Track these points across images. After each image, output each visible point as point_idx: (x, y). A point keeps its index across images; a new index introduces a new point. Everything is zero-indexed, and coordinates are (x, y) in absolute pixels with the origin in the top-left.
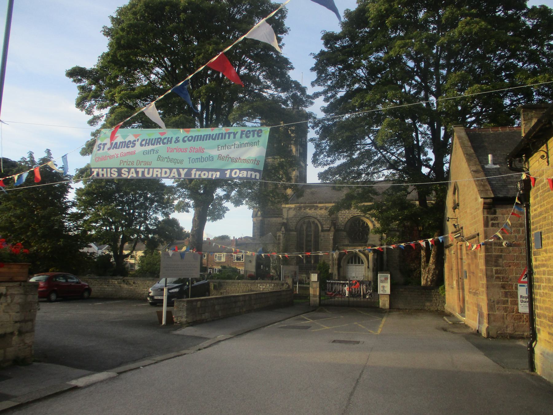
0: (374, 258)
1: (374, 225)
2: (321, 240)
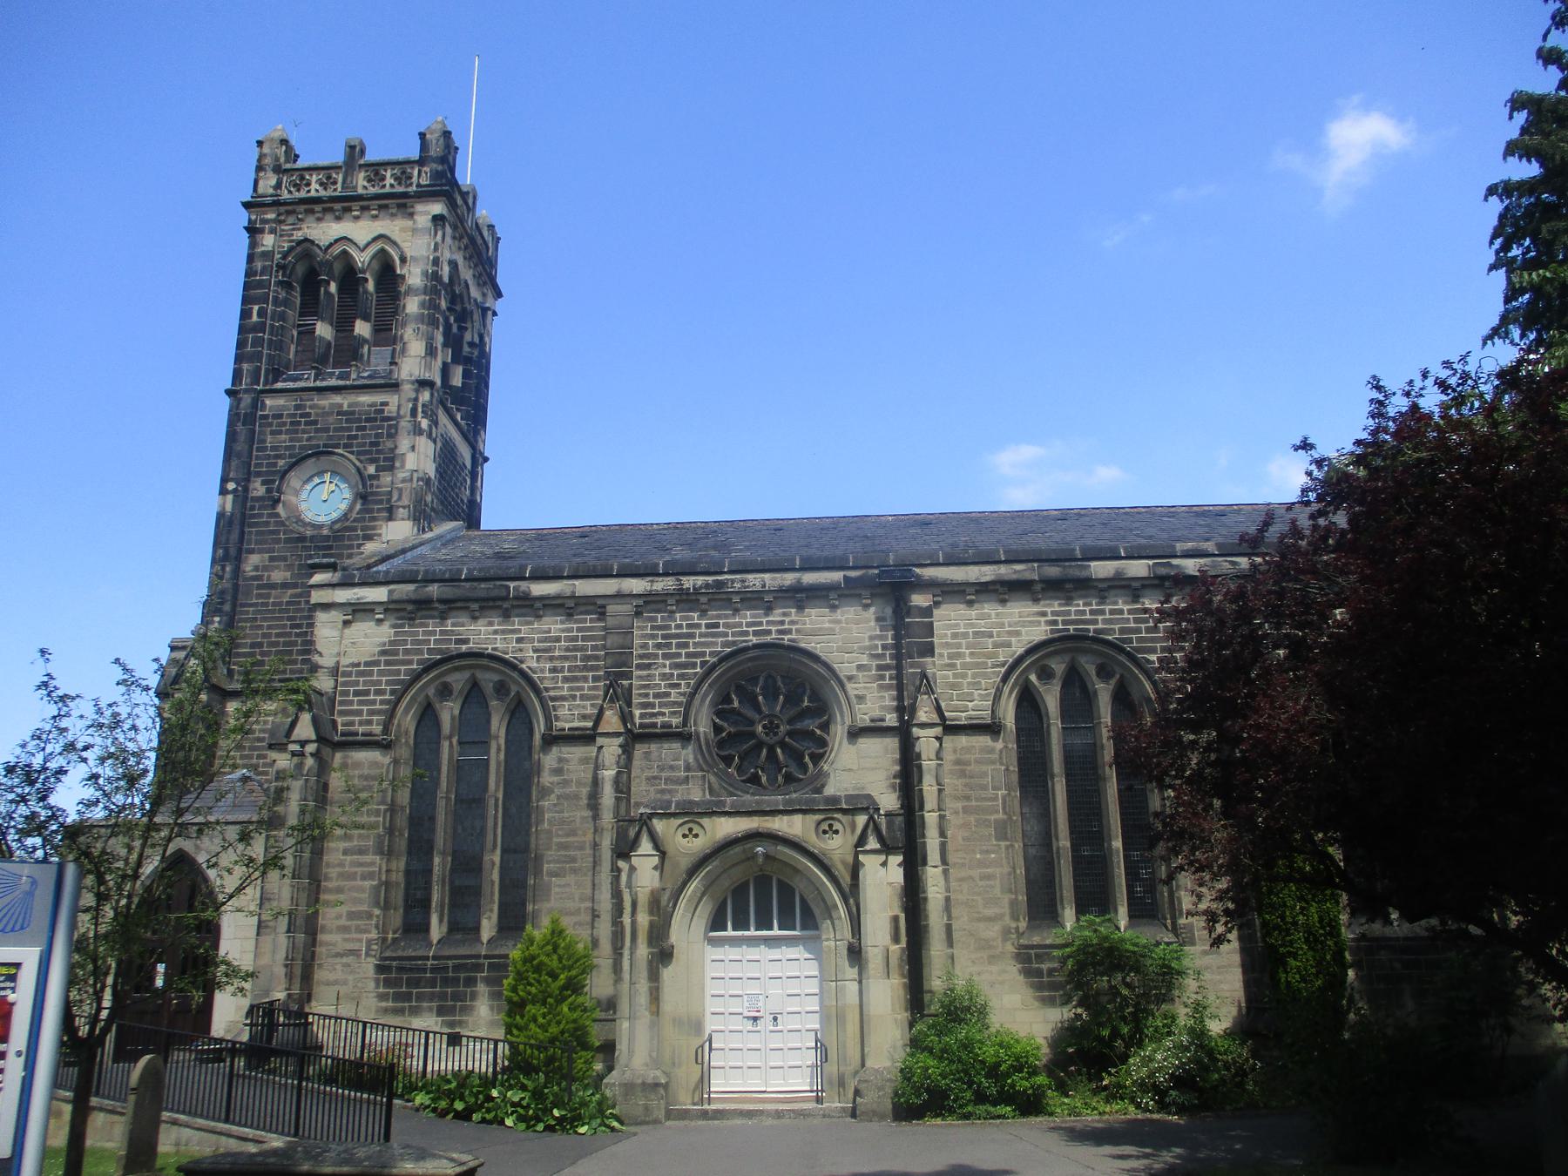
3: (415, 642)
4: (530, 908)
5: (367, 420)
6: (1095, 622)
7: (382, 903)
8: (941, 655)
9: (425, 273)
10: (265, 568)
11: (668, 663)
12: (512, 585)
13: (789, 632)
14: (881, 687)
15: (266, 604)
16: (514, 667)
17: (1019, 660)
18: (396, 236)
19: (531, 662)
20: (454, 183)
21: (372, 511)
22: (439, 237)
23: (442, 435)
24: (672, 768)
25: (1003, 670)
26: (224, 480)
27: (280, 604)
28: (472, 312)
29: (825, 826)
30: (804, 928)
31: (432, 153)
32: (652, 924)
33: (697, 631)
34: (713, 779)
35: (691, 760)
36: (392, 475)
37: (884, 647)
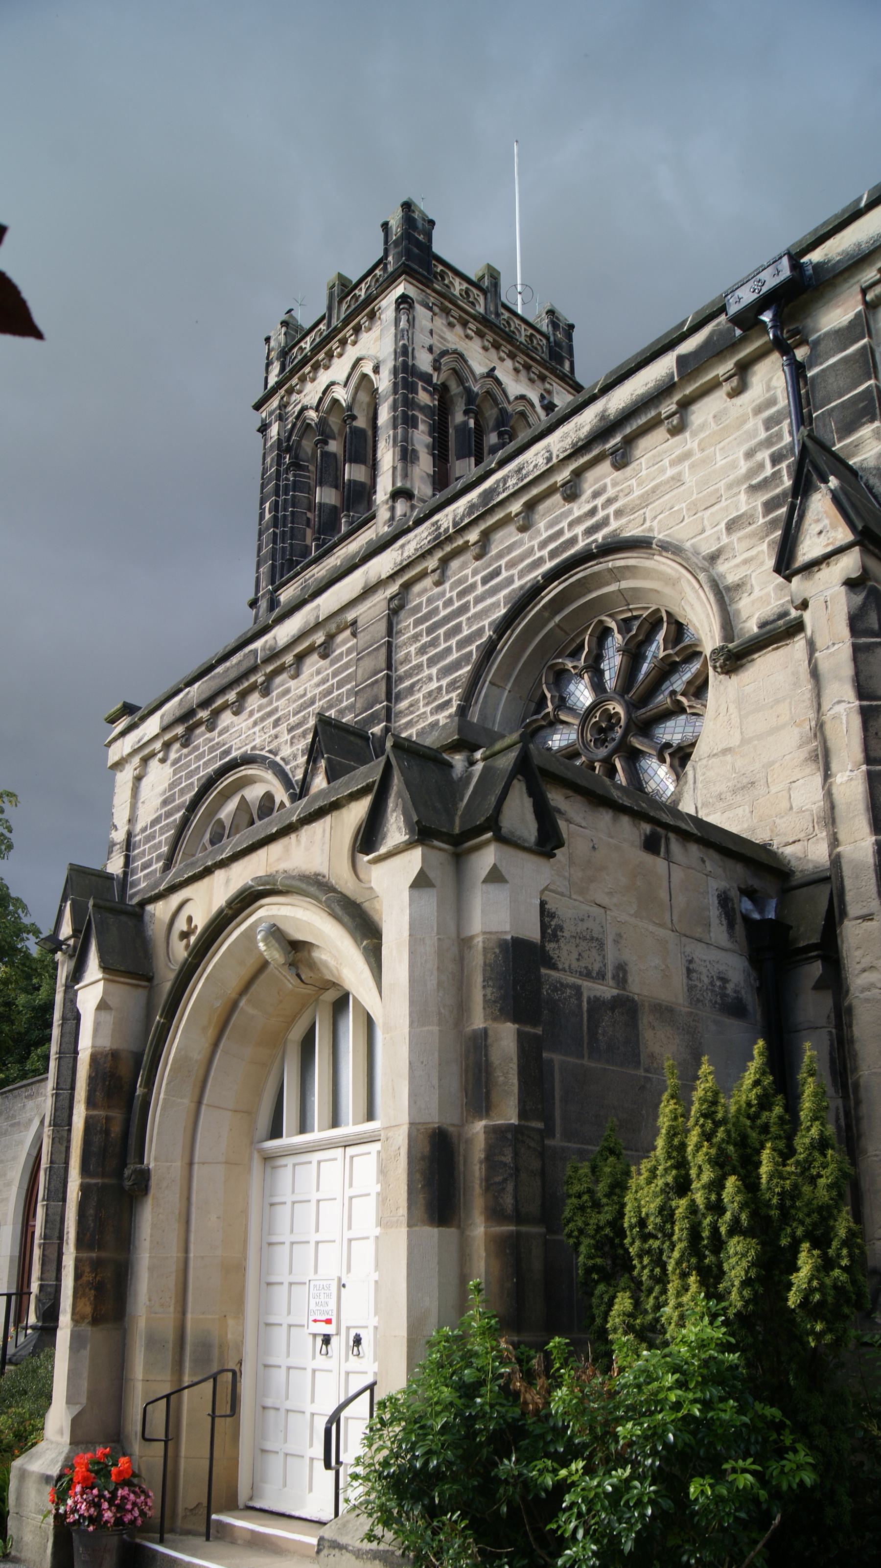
12: (258, 644)
13: (605, 522)
18: (372, 352)
28: (522, 414)
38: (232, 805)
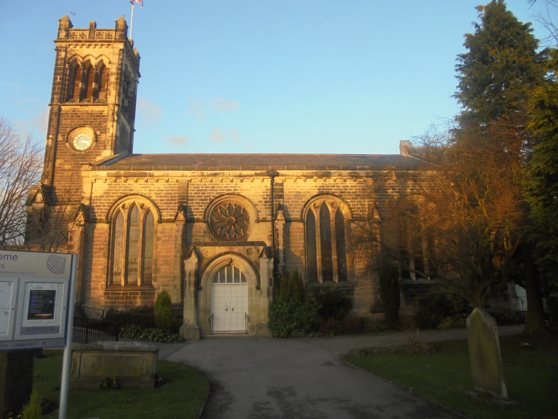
0: (269, 269)
1: (258, 212)
2: (158, 239)
3: (115, 190)
4: (153, 275)
5: (97, 116)
6: (332, 189)
7: (106, 274)
8: (285, 199)
9: (118, 69)
10: (63, 164)
11: (198, 198)
12: (148, 172)
14: (266, 208)
15: (63, 176)
16: (148, 198)
17: (309, 200)
18: (107, 55)
19: (154, 198)
20: (126, 38)
21: (99, 147)
22: (121, 57)
23: (121, 122)
24: (200, 232)
25: (304, 203)
26: (48, 134)
27: (68, 176)
28: (131, 82)
29: (249, 251)
30: (242, 282)
31: (120, 28)
32: (195, 280)
33: (208, 189)
34: (213, 236)
35: (206, 230)
36: (106, 135)
37: (267, 195)
38: (131, 201)
